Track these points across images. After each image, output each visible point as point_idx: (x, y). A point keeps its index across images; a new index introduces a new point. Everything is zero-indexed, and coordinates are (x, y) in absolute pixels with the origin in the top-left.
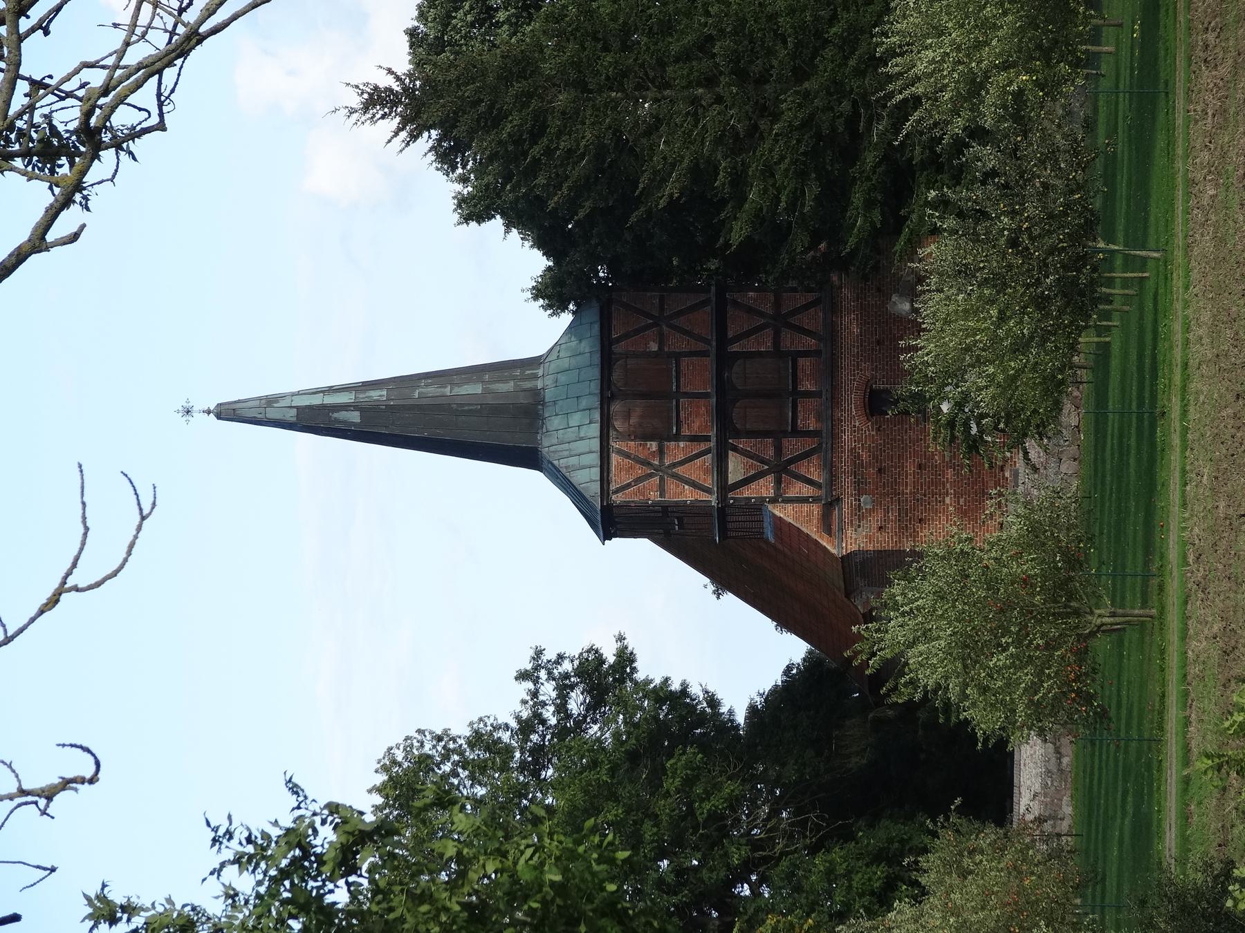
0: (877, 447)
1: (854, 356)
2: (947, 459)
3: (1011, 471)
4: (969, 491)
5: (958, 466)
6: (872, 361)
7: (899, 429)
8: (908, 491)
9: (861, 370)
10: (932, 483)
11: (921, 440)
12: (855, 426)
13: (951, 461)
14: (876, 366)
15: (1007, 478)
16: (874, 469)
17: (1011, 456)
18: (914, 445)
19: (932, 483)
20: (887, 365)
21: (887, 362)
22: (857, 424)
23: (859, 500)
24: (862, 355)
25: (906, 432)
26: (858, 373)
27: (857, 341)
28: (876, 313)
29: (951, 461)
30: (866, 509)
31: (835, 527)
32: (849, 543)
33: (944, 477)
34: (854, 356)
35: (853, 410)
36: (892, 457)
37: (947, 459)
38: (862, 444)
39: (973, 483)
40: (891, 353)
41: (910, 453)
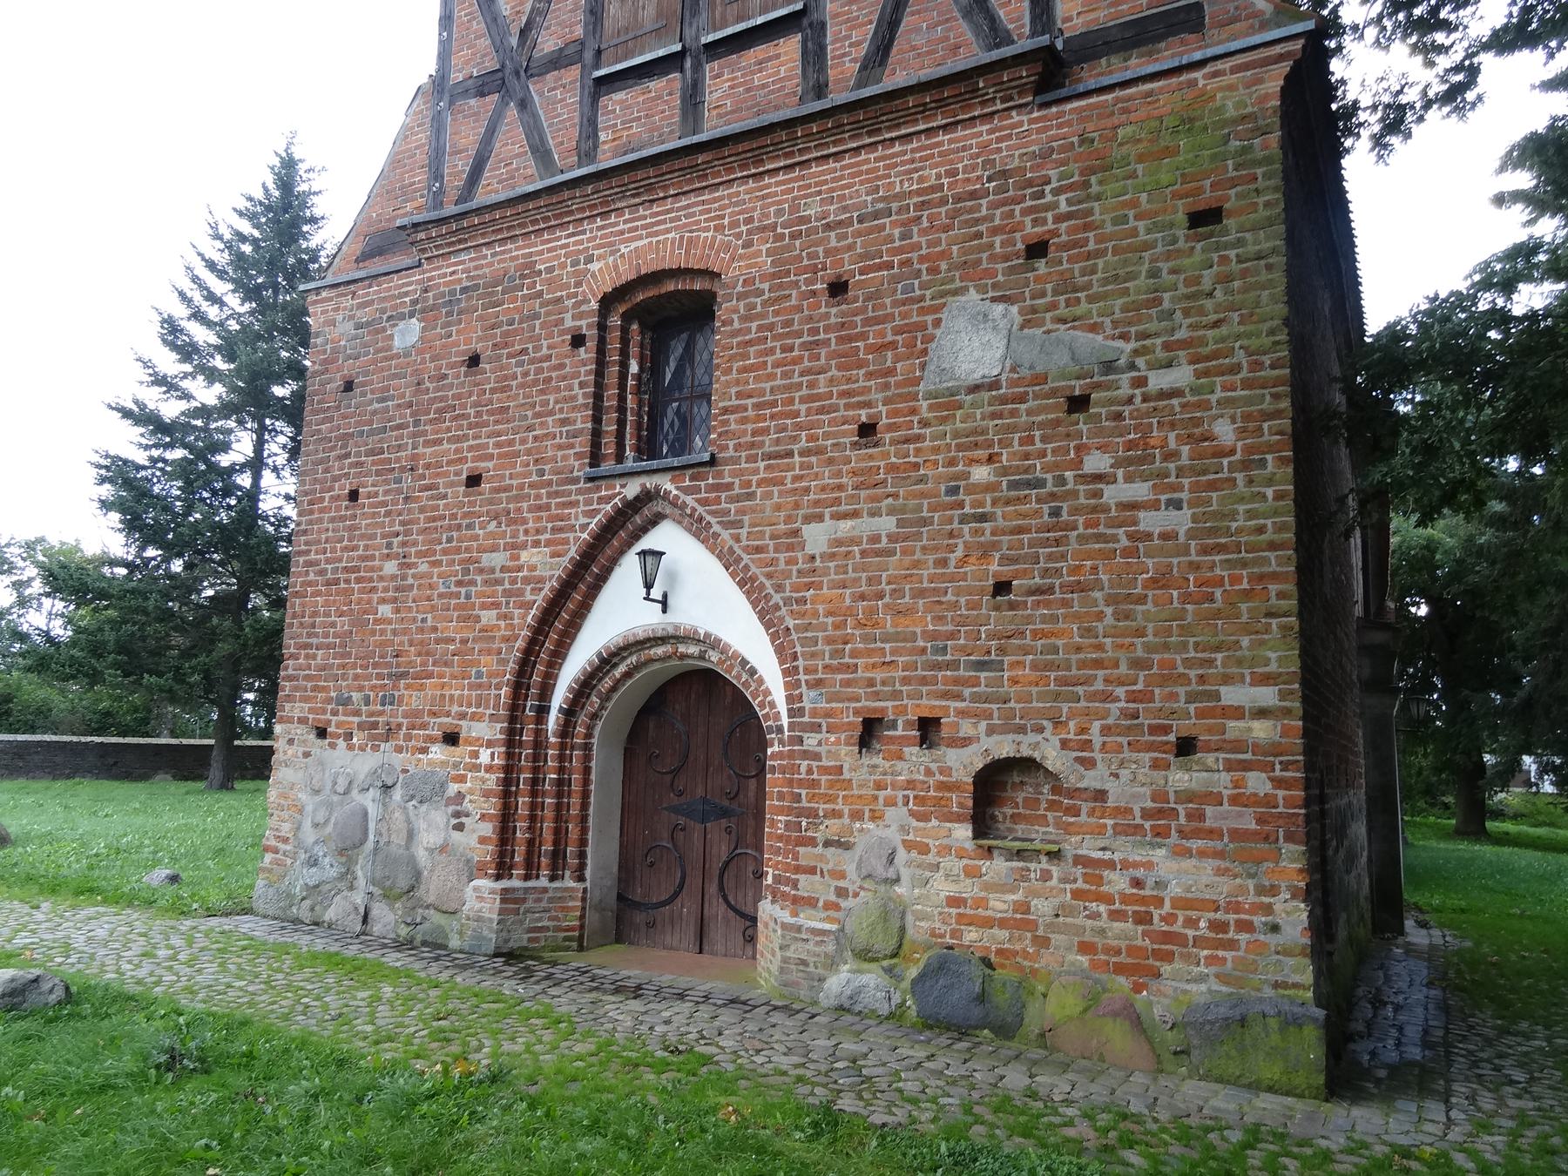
0: (531, 339)
1: (795, 208)
2: (487, 559)
3: (444, 764)
4: (405, 632)
5: (468, 596)
6: (774, 276)
7: (573, 398)
8: (420, 450)
9: (748, 244)
10: (434, 519)
11: (541, 473)
12: (590, 260)
13: (481, 571)
14: (760, 293)
15: (424, 751)
16: (480, 339)
17: (477, 768)
18: (529, 452)
19: (434, 519)
20: (760, 328)
21: (771, 327)
22: (595, 266)
23: (412, 315)
24: (793, 236)
25: (564, 422)
26: (738, 236)
27: (845, 209)
28: (944, 255)
29: (481, 571)
30: (392, 336)
31: (377, 266)
32: (330, 306)
33: (445, 552)
34: (795, 208)
35: (633, 245)
36: (503, 390)
37: (487, 559)
38: (540, 294)
39: (422, 643)
40: (799, 334)
41: (511, 443)
